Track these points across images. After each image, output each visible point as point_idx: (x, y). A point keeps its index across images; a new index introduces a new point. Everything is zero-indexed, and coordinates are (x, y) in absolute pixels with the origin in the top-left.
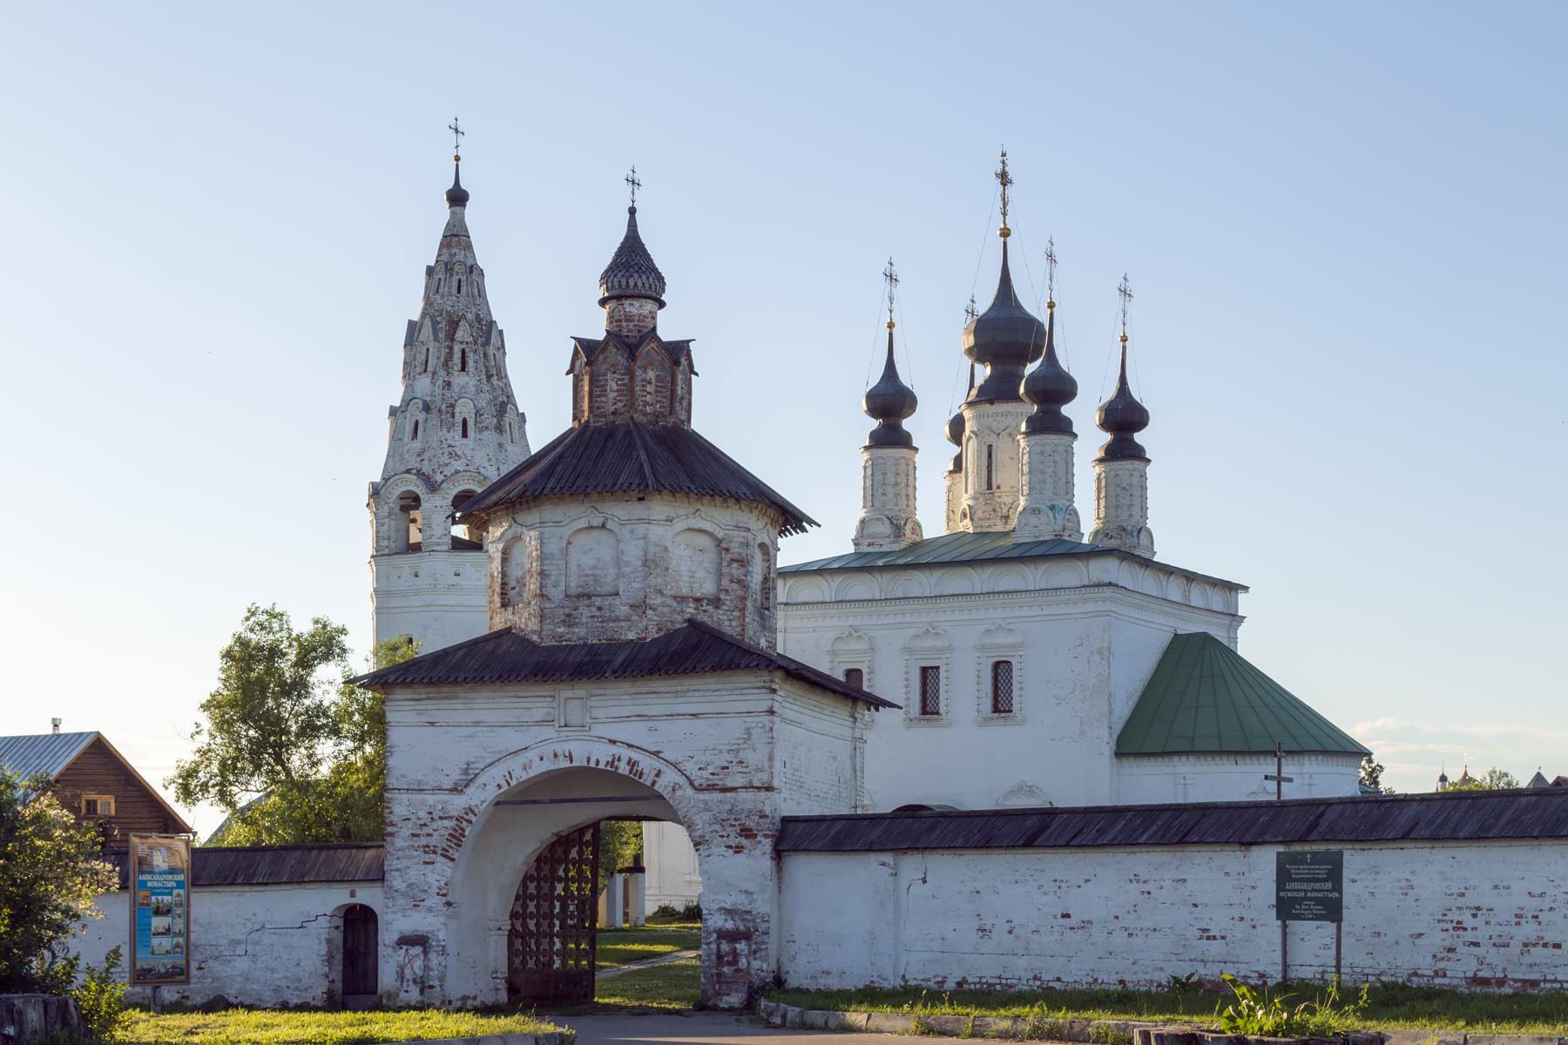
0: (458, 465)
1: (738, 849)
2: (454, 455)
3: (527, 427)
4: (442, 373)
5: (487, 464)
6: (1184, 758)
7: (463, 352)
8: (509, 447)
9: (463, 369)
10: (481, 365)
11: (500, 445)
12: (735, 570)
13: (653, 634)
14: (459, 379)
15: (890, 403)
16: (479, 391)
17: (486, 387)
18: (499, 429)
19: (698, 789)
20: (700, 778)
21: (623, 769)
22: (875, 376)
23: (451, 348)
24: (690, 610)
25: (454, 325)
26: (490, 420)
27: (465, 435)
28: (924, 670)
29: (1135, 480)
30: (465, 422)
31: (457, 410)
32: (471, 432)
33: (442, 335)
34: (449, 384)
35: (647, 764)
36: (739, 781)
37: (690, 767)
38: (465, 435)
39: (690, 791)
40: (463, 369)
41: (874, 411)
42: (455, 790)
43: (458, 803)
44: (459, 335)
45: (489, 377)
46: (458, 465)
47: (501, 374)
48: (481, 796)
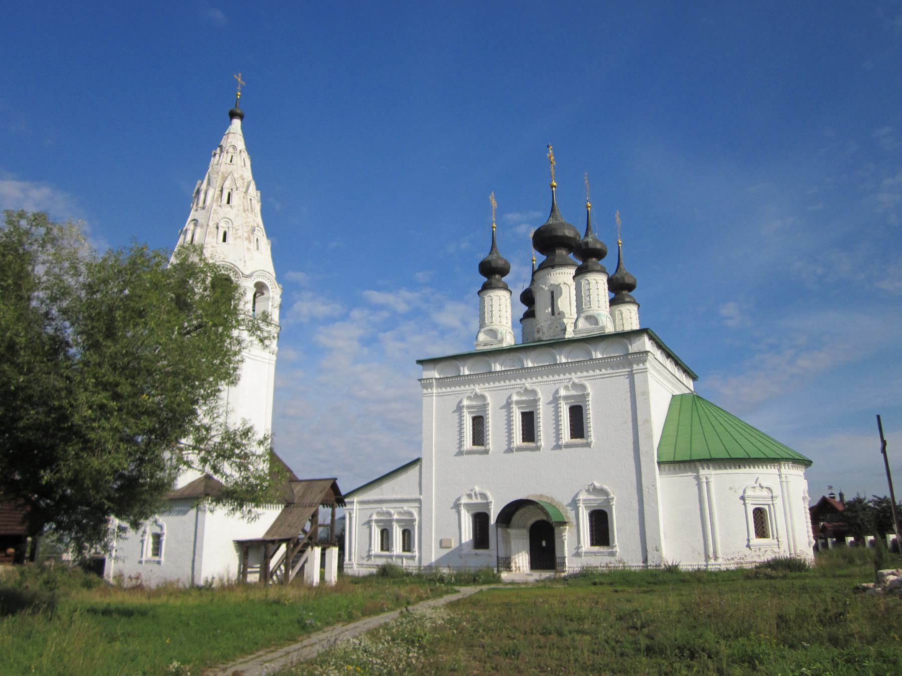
14: (227, 209)
18: (249, 239)
25: (225, 179)
26: (244, 232)
27: (224, 240)
38: (224, 240)
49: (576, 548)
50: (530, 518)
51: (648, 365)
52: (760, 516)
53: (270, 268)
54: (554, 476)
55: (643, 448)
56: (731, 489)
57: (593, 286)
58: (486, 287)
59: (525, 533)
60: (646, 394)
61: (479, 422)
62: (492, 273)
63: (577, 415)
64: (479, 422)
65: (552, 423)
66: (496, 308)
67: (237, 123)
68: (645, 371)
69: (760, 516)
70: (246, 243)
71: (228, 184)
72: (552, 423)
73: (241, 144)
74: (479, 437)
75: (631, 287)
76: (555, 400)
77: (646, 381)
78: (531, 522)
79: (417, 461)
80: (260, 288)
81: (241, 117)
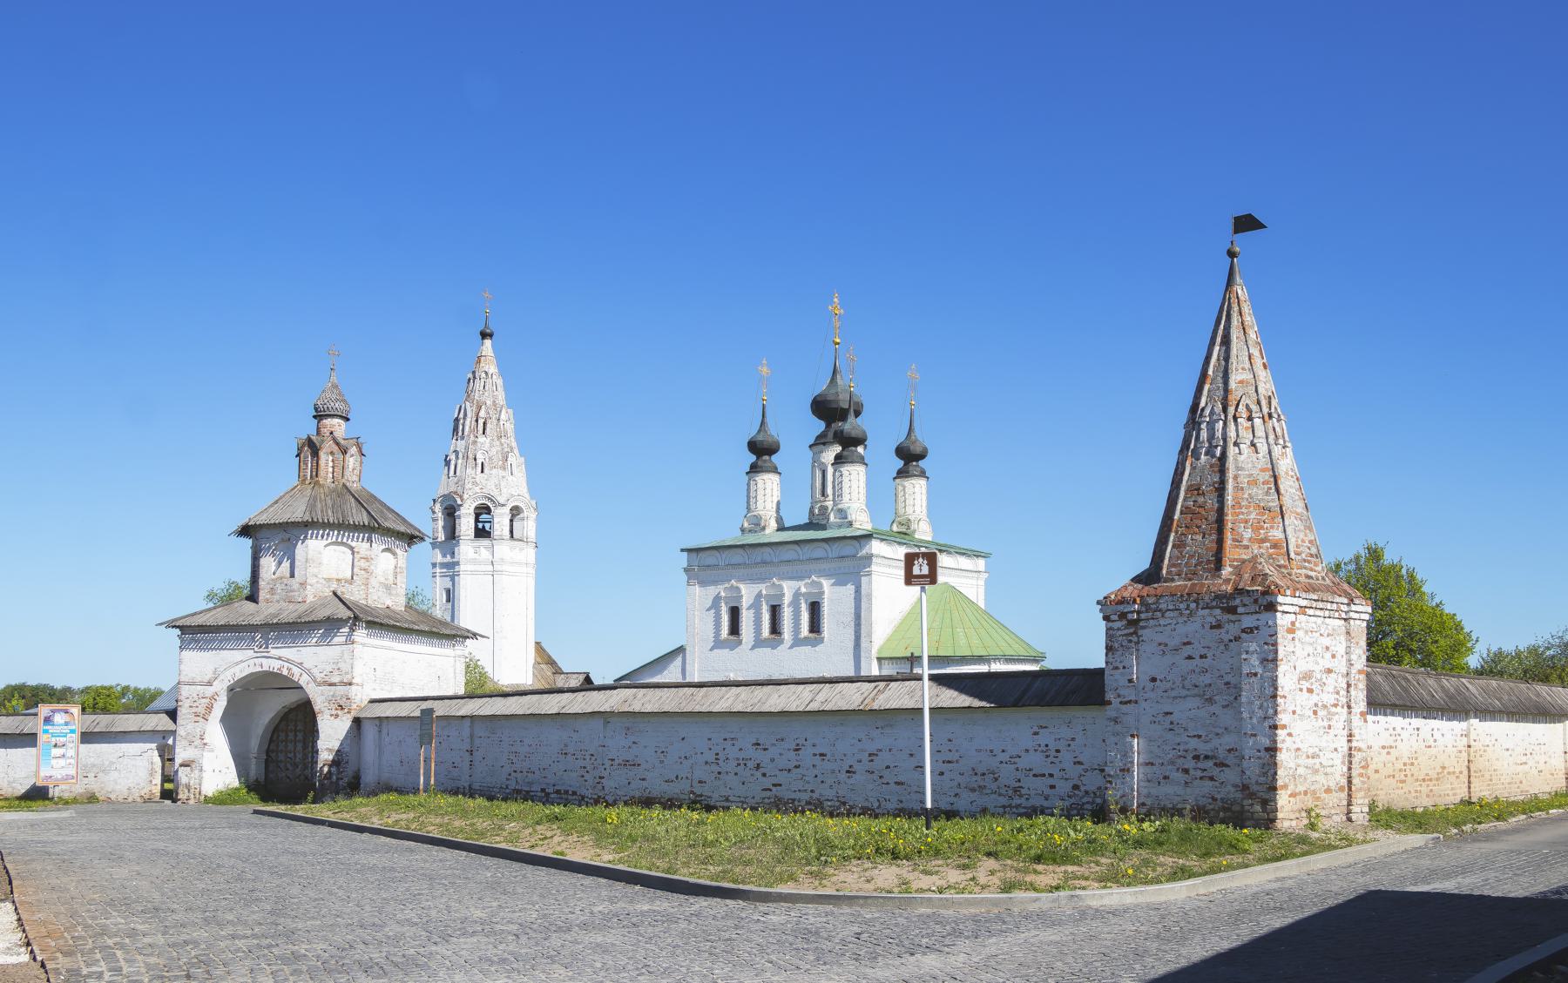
0: (477, 489)
1: (337, 716)
2: (474, 483)
12: (363, 564)
13: (310, 599)
14: (481, 439)
19: (319, 685)
20: (319, 677)
21: (285, 672)
24: (334, 586)
25: (479, 408)
35: (296, 670)
36: (336, 679)
37: (315, 672)
39: (312, 685)
42: (210, 684)
43: (209, 691)
46: (477, 489)
48: (221, 687)
51: (874, 567)
53: (524, 490)
55: (864, 644)
57: (845, 479)
58: (754, 469)
60: (869, 596)
61: (735, 613)
62: (762, 451)
63: (815, 609)
64: (735, 613)
65: (795, 621)
66: (761, 492)
67: (488, 342)
68: (869, 574)
70: (502, 473)
71: (482, 414)
72: (795, 621)
73: (493, 369)
74: (735, 629)
75: (921, 456)
76: (797, 595)
77: (870, 582)
79: (680, 650)
80: (515, 511)
81: (491, 335)
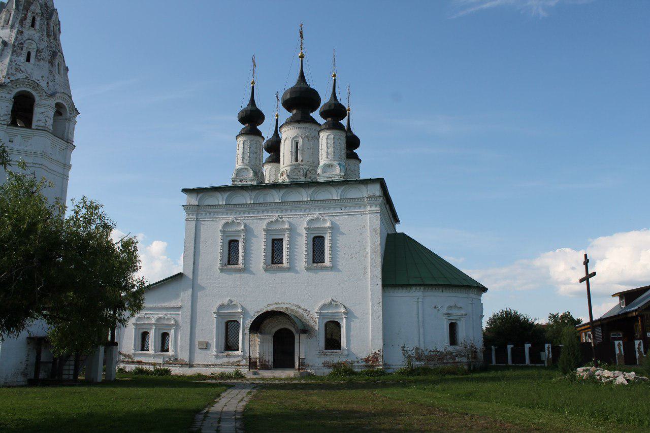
0: (20, 76)
3: (69, 74)
4: (17, 26)
5: (40, 79)
6: (418, 288)
7: (34, 19)
8: (57, 76)
9: (33, 25)
10: (44, 27)
11: (51, 71)
14: (32, 32)
15: (251, 118)
16: (41, 39)
17: (45, 39)
18: (51, 62)
22: (245, 103)
23: (26, 15)
26: (45, 55)
27: (28, 60)
28: (273, 240)
29: (356, 168)
30: (29, 54)
31: (25, 45)
32: (32, 60)
33: (21, 8)
34: (22, 32)
38: (28, 60)
40: (33, 25)
41: (242, 120)
44: (32, 8)
45: (49, 36)
47: (56, 39)
49: (309, 353)
50: (275, 326)
52: (453, 327)
54: (301, 292)
56: (435, 307)
59: (270, 339)
69: (453, 327)
78: (274, 330)
